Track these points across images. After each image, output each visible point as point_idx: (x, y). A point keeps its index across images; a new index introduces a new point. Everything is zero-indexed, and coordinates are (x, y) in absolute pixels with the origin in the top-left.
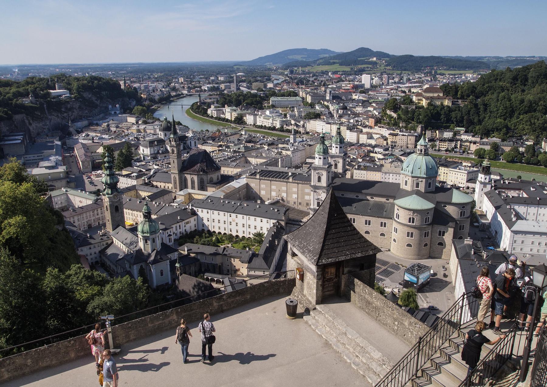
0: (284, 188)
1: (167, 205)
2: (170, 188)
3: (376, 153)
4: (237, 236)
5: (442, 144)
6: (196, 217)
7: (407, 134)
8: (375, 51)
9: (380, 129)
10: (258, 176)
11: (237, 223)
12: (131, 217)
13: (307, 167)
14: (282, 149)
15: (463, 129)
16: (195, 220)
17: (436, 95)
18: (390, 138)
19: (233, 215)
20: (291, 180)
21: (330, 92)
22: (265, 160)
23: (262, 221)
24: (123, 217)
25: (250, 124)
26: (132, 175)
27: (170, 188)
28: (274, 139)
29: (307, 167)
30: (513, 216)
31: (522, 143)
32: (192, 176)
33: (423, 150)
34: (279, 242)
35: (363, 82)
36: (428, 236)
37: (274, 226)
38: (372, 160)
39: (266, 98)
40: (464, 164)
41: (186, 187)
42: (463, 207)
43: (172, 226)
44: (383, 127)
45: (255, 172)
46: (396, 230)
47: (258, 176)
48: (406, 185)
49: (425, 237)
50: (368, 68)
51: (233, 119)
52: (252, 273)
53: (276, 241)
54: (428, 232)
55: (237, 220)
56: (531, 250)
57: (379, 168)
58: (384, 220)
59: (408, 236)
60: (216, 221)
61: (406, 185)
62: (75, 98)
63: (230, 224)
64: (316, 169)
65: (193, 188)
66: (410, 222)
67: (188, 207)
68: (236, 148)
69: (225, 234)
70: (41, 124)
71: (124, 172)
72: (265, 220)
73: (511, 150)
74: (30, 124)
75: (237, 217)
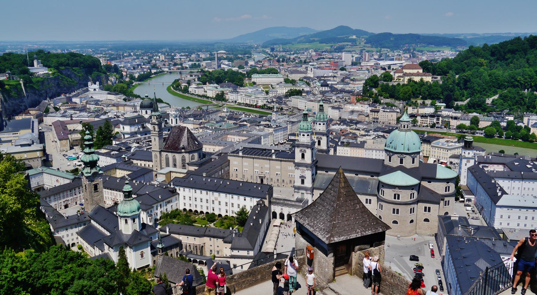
0: (267, 166)
1: (148, 184)
2: (151, 166)
3: (358, 130)
4: (220, 215)
5: (424, 120)
6: (177, 196)
7: (388, 110)
8: (354, 27)
9: (362, 105)
10: (241, 154)
11: (220, 202)
12: (110, 196)
13: (289, 144)
14: (265, 127)
15: (444, 104)
17: (415, 71)
18: (372, 114)
19: (216, 194)
20: (274, 157)
21: (311, 69)
22: (246, 138)
23: (245, 200)
24: (102, 196)
25: (231, 101)
26: (112, 153)
27: (151, 166)
28: (256, 116)
29: (289, 144)
30: (498, 191)
31: (503, 117)
32: (173, 154)
33: (406, 126)
35: (343, 60)
36: (413, 212)
37: (258, 204)
38: (355, 137)
39: (249, 75)
40: (447, 139)
41: (168, 165)
42: (448, 183)
43: (153, 206)
44: (364, 104)
45: (238, 150)
47: (241, 154)
48: (390, 161)
49: (411, 213)
50: (348, 45)
51: (214, 96)
52: (235, 253)
53: (260, 220)
54: (414, 208)
55: (219, 199)
56: (518, 225)
57: (362, 145)
59: (394, 213)
61: (390, 161)
62: (53, 74)
63: (213, 203)
65: (175, 166)
66: (395, 198)
67: (169, 186)
68: (217, 126)
69: (207, 213)
70: (17, 101)
71: (103, 151)
72: (248, 199)
73: (491, 126)
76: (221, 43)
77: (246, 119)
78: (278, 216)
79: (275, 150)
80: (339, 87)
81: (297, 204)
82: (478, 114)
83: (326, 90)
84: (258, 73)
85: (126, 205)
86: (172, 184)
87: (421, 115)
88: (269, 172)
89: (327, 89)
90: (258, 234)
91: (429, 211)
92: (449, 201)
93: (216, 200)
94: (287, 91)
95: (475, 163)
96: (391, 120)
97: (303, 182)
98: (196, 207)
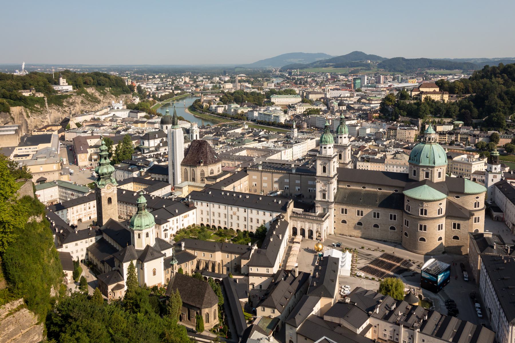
5: (442, 137)
6: (194, 210)
7: (406, 128)
8: (368, 53)
10: (260, 168)
16: (193, 214)
19: (235, 209)
34: (283, 237)
36: (442, 229)
46: (407, 223)
47: (260, 168)
49: (439, 229)
54: (442, 225)
55: (238, 214)
57: (382, 161)
58: (393, 212)
60: (216, 215)
63: (232, 218)
64: (321, 158)
69: (225, 228)
72: (268, 214)
74: (28, 117)
75: (238, 210)
76: (241, 68)
77: (265, 135)
78: (299, 232)
79: (295, 165)
80: (356, 106)
81: (319, 219)
82: (497, 132)
83: (343, 109)
84: (276, 93)
85: (139, 218)
86: (190, 197)
87: (439, 133)
88: (288, 186)
89: (344, 108)
90: (278, 251)
91: (459, 228)
92: (479, 218)
93: (235, 214)
94: (305, 110)
95: (502, 179)
96: (408, 138)
97: (324, 196)
98: (214, 222)
